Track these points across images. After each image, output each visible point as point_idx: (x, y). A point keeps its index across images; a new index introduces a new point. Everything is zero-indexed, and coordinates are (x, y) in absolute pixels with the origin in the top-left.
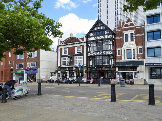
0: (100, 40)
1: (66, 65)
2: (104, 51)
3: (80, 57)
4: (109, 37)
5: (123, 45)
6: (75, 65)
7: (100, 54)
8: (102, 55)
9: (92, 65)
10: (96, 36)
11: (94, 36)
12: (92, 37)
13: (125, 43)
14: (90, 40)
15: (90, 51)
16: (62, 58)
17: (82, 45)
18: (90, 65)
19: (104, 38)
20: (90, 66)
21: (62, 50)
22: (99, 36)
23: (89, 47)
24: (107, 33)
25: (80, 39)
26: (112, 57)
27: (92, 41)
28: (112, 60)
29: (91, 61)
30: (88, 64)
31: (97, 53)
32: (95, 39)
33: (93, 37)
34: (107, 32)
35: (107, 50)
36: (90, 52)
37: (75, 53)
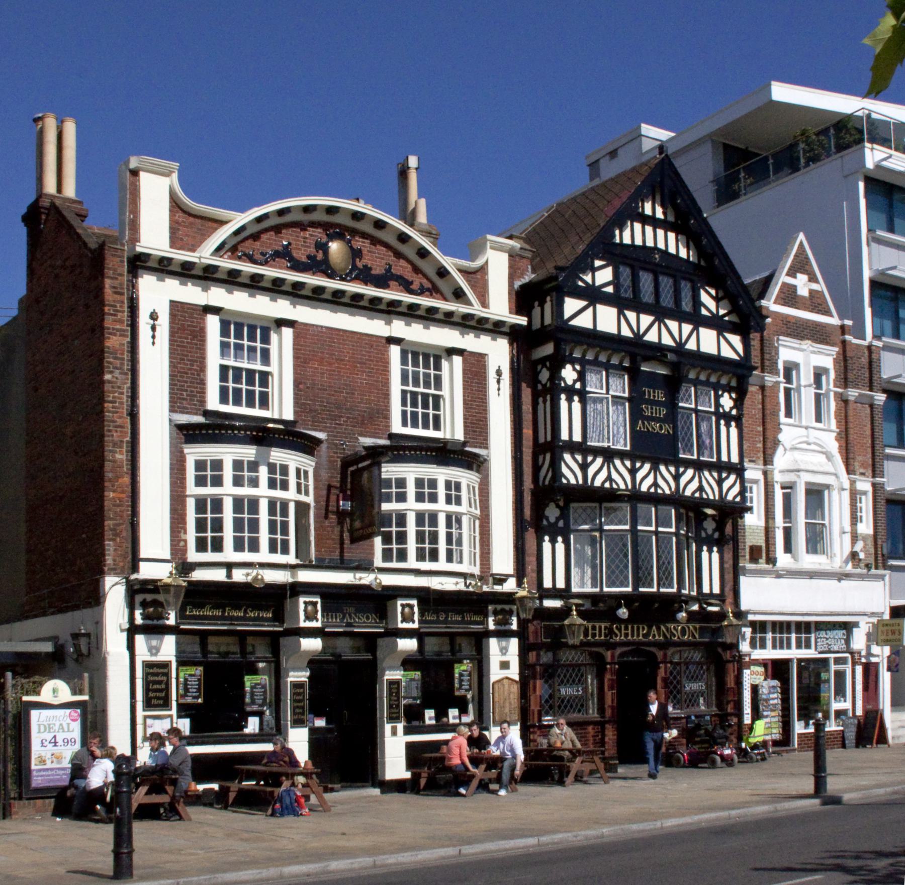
0: (657, 351)
1: (218, 546)
2: (688, 464)
3: (442, 474)
4: (727, 353)
5: (777, 443)
6: (418, 572)
7: (655, 484)
8: (676, 500)
9: (561, 584)
10: (640, 308)
11: (620, 302)
12: (593, 296)
13: (788, 434)
14: (584, 321)
15: (577, 437)
16: (194, 453)
17: (470, 348)
18: (547, 584)
19: (691, 345)
20: (554, 593)
21: (200, 335)
22: (660, 314)
23: (570, 392)
24: (714, 310)
25: (487, 263)
26: (710, 532)
27: (593, 337)
28: (710, 551)
29: (553, 542)
30: (531, 567)
31: (633, 472)
32: (626, 332)
33: (608, 300)
34: (711, 304)
35: (710, 466)
36: (572, 447)
37: (387, 417)
